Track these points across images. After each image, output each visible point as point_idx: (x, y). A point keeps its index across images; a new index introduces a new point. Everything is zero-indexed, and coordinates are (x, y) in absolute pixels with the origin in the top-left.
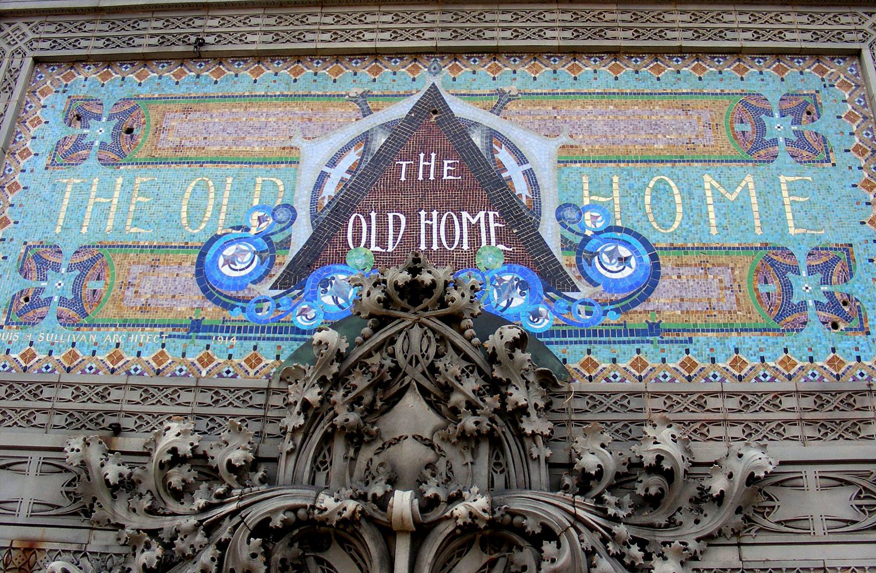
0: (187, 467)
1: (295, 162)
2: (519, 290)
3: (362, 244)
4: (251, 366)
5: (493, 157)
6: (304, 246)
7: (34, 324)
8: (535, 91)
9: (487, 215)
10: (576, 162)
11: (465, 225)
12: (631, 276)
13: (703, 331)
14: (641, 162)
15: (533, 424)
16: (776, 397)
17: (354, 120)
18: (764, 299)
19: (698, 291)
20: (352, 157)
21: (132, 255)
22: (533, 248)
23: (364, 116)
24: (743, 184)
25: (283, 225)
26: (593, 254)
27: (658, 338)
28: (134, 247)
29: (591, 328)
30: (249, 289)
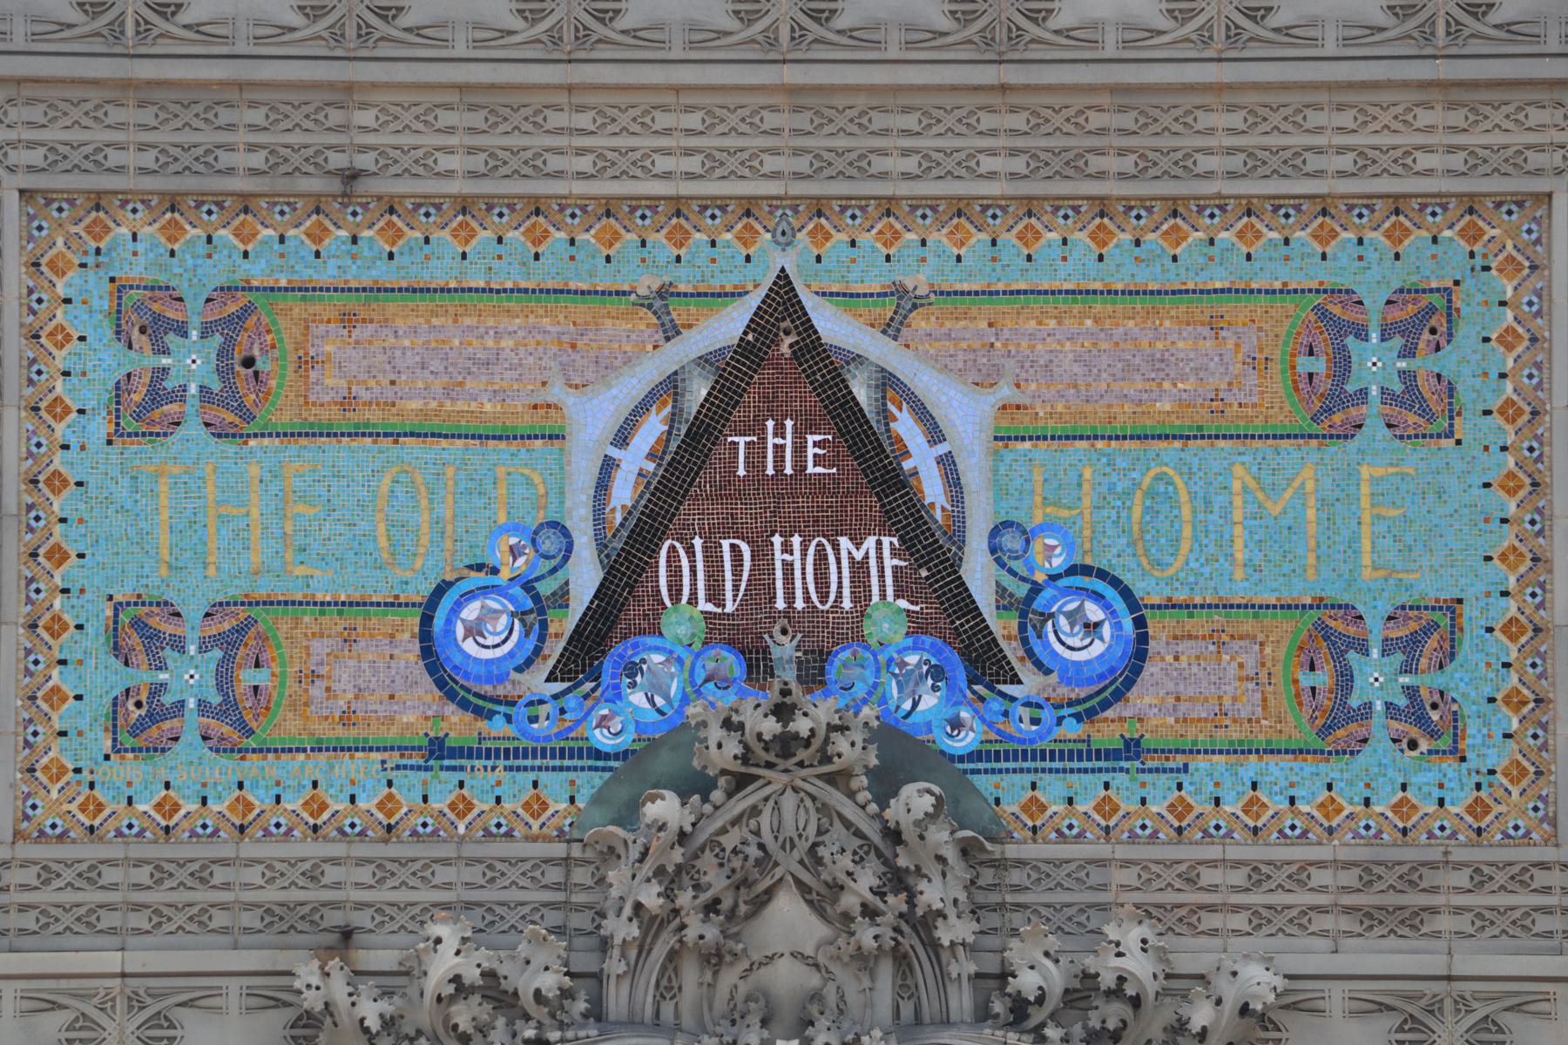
0: (476, 998)
1: (557, 437)
2: (930, 682)
3: (685, 599)
4: (532, 815)
5: (888, 430)
6: (592, 602)
7: (163, 750)
8: (958, 287)
9: (879, 543)
10: (1023, 439)
11: (845, 563)
12: (1102, 655)
13: (1206, 752)
14: (1132, 437)
16: (1302, 869)
17: (650, 347)
18: (1306, 698)
19: (1204, 684)
20: (653, 428)
21: (307, 619)
22: (951, 606)
23: (668, 339)
24: (1296, 484)
25: (554, 563)
26: (1047, 616)
27: (1137, 764)
28: (308, 604)
29: (1039, 746)
30: (513, 682)
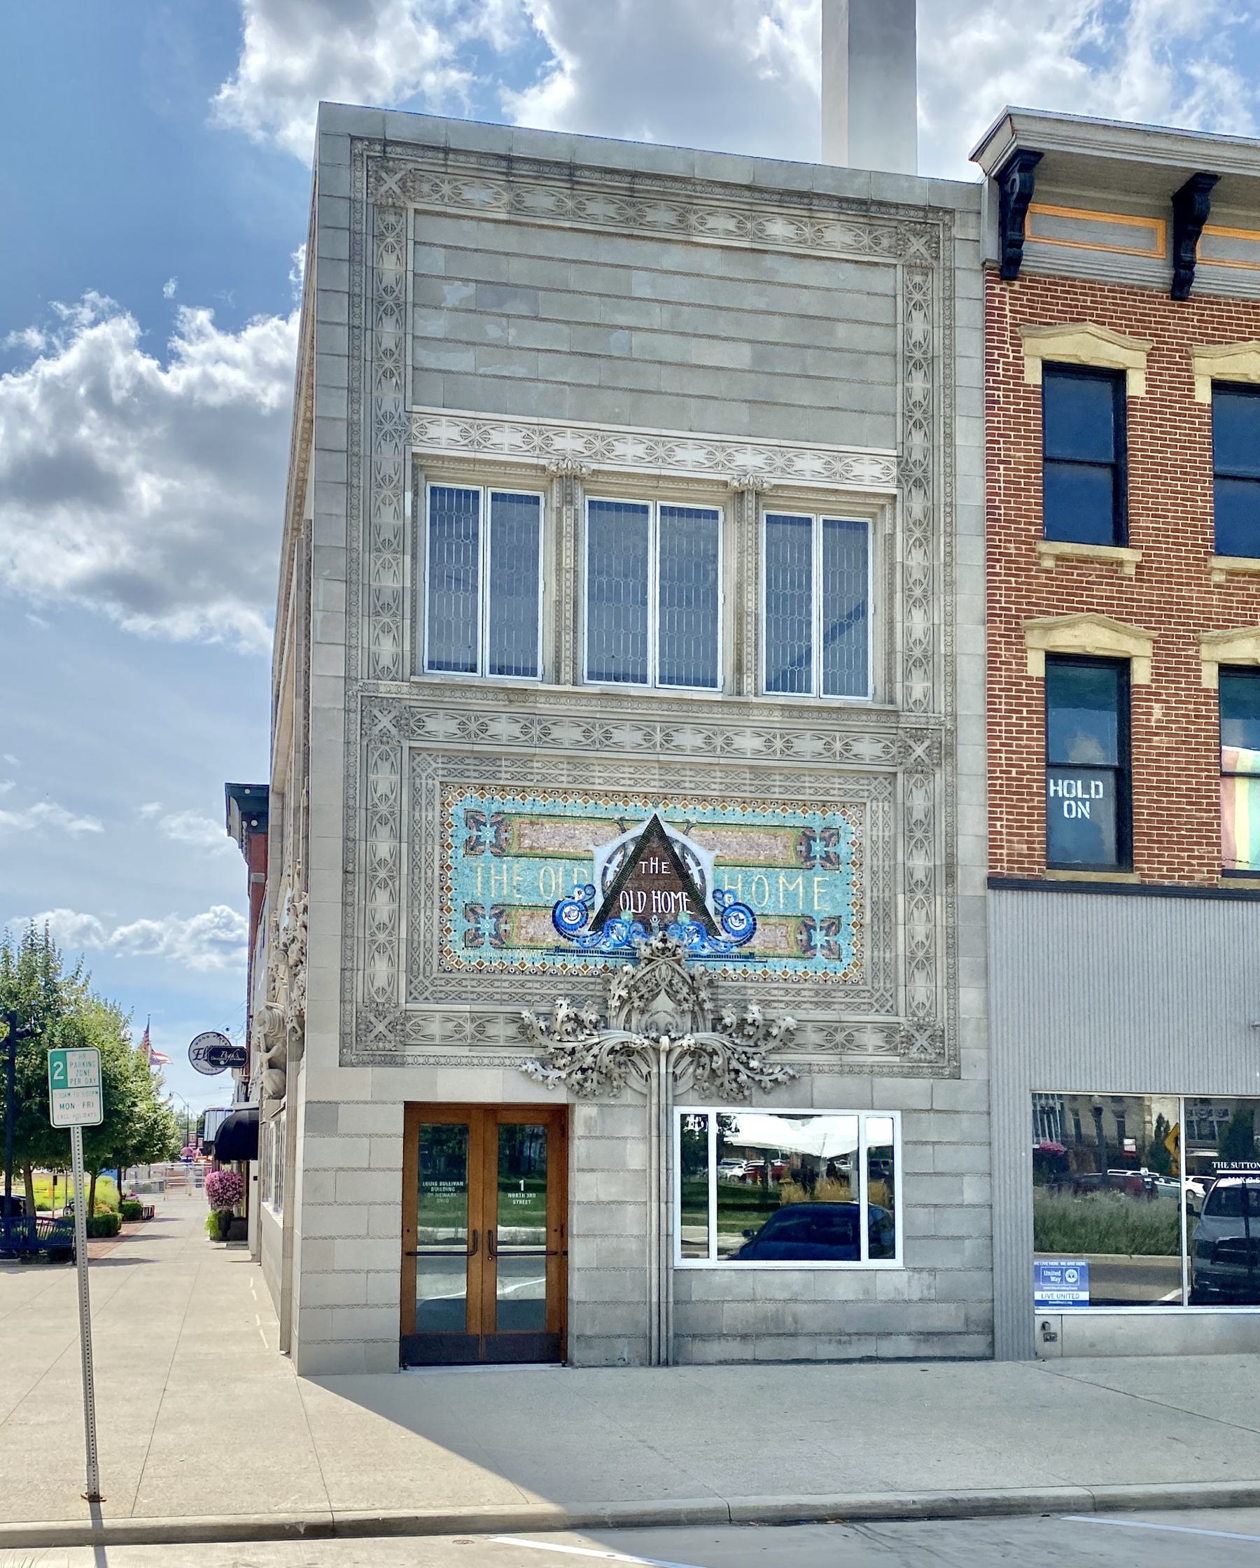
15: (707, 1006)
20: (619, 858)
